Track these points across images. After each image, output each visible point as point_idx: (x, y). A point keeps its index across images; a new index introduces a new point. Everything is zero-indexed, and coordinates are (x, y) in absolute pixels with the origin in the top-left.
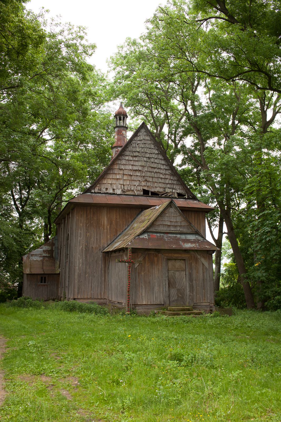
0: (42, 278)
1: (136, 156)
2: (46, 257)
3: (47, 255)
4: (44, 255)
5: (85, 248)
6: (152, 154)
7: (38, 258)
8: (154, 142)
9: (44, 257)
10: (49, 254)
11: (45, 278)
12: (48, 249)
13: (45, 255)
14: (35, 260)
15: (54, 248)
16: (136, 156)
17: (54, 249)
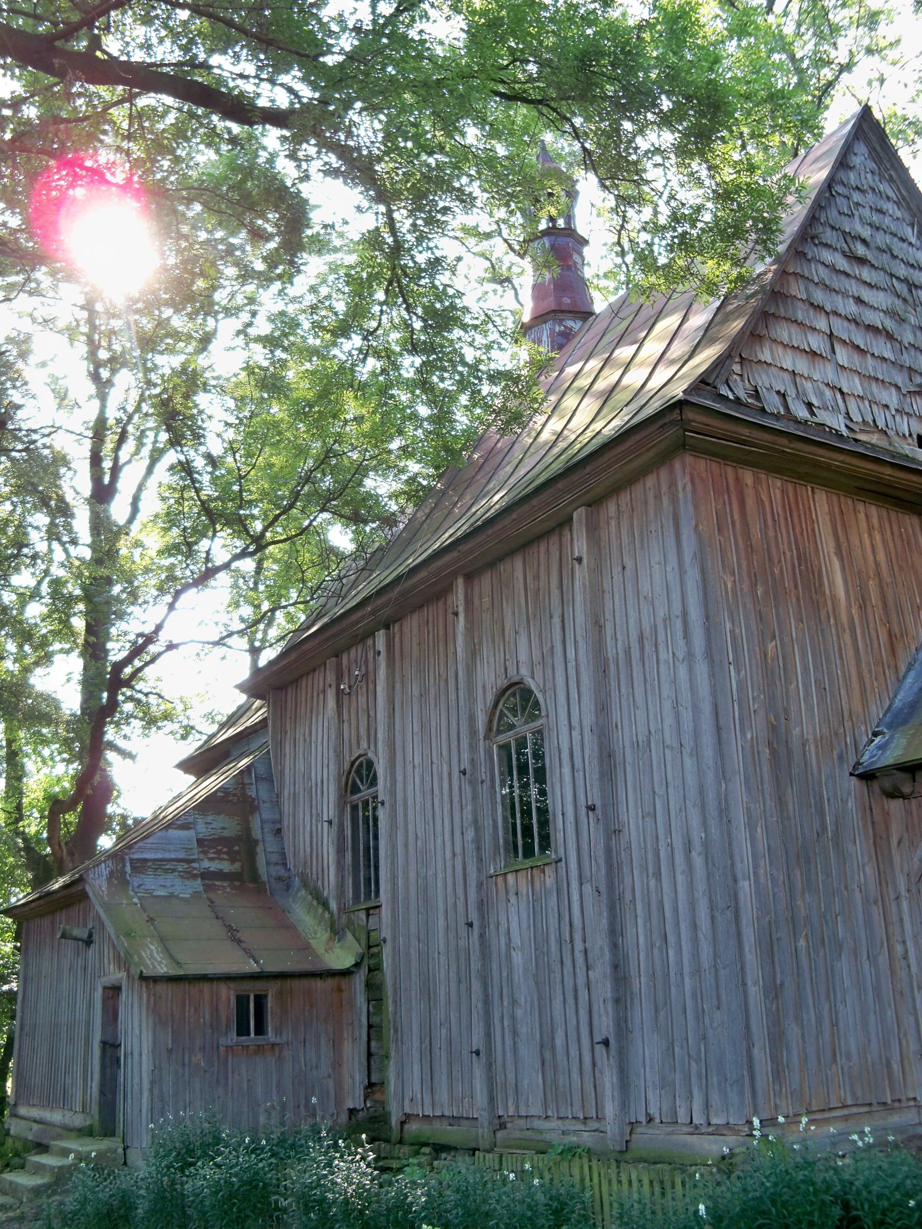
0: (242, 1001)
1: (862, 261)
2: (220, 875)
3: (226, 866)
4: (206, 864)
5: (770, 744)
6: (912, 266)
7: (178, 882)
8: (913, 215)
9: (206, 875)
10: (233, 861)
11: (260, 1001)
12: (226, 834)
13: (214, 866)
14: (161, 893)
15: (256, 823)
16: (862, 261)
17: (257, 834)
